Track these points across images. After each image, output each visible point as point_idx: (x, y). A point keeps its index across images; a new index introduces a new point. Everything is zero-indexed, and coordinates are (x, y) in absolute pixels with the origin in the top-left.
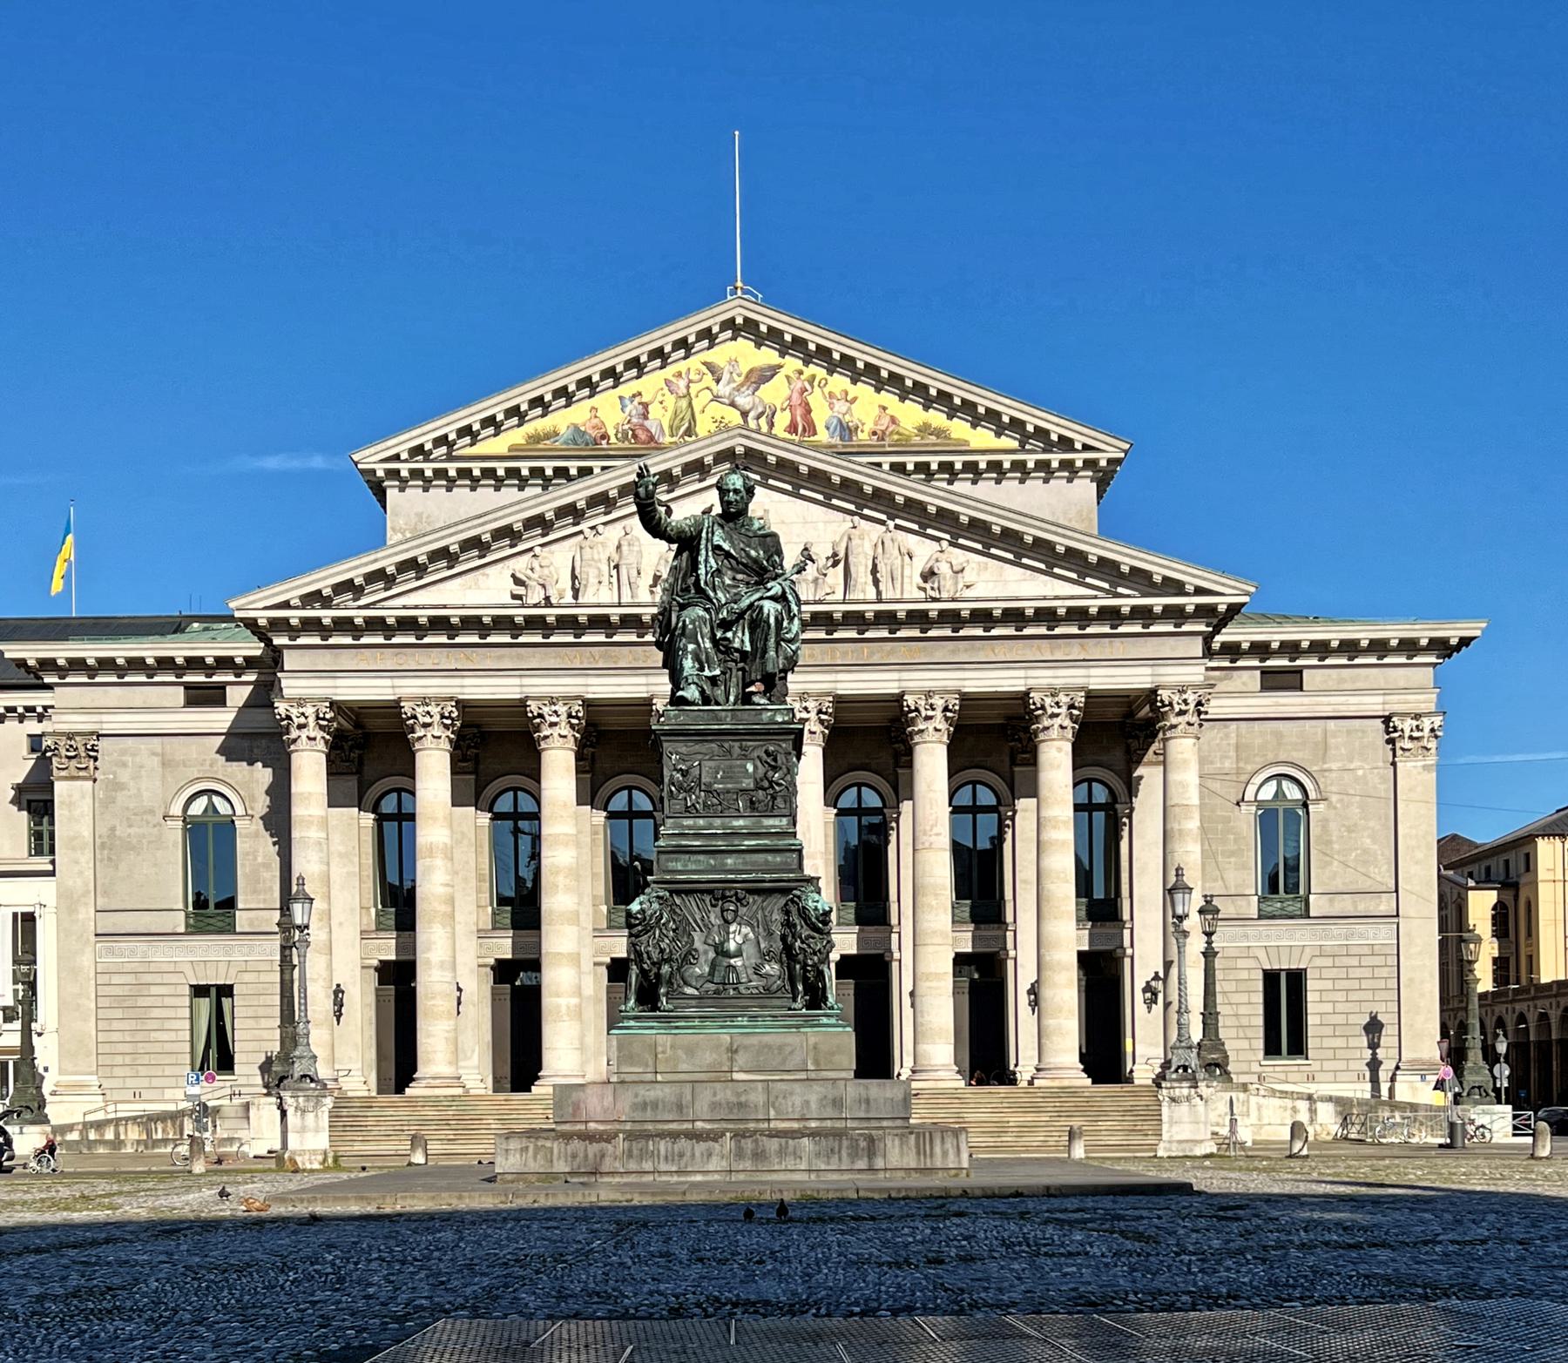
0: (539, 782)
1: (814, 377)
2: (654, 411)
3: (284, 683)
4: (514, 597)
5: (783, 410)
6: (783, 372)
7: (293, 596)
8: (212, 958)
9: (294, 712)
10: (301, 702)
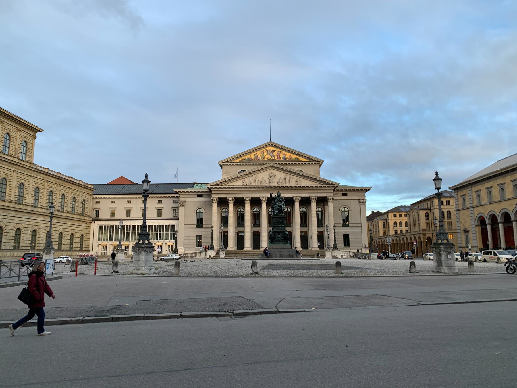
0: (245, 207)
2: (259, 156)
7: (214, 184)
8: (200, 231)
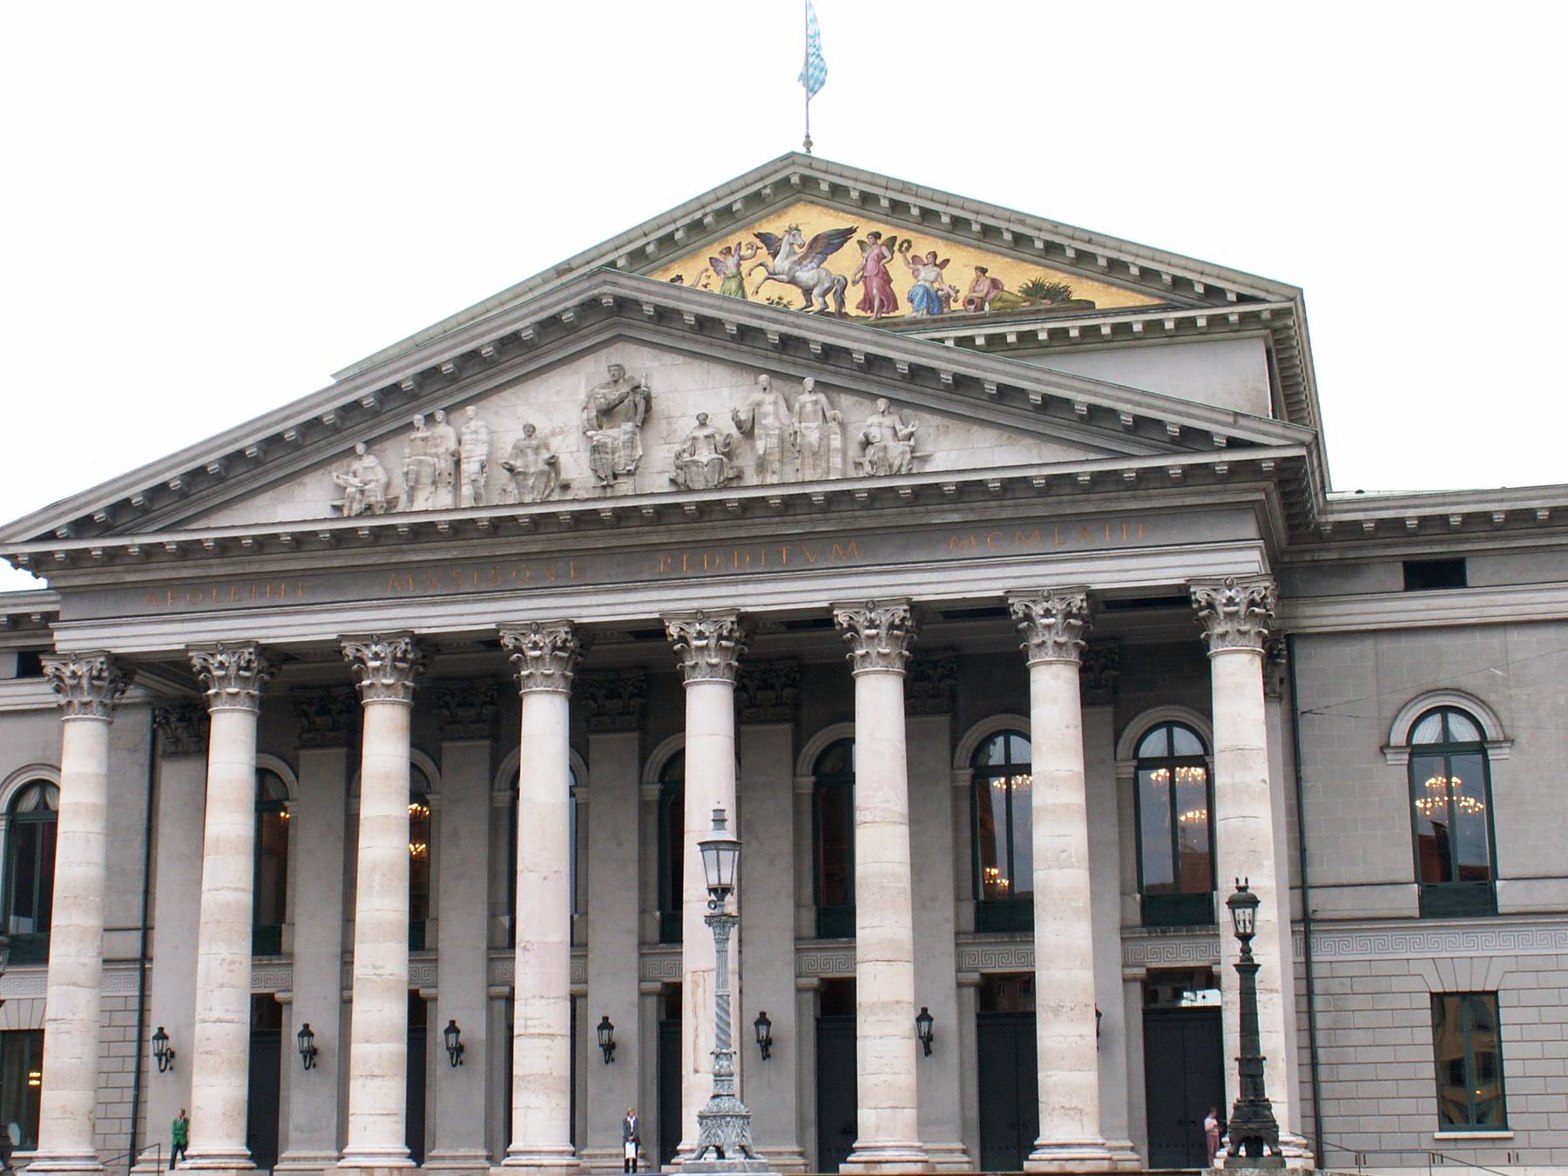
1: (895, 238)
3: (57, 636)
4: (337, 508)
5: (855, 283)
6: (856, 237)
9: (67, 672)
10: (77, 657)
